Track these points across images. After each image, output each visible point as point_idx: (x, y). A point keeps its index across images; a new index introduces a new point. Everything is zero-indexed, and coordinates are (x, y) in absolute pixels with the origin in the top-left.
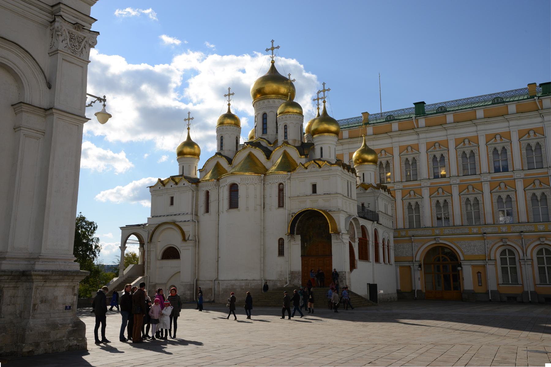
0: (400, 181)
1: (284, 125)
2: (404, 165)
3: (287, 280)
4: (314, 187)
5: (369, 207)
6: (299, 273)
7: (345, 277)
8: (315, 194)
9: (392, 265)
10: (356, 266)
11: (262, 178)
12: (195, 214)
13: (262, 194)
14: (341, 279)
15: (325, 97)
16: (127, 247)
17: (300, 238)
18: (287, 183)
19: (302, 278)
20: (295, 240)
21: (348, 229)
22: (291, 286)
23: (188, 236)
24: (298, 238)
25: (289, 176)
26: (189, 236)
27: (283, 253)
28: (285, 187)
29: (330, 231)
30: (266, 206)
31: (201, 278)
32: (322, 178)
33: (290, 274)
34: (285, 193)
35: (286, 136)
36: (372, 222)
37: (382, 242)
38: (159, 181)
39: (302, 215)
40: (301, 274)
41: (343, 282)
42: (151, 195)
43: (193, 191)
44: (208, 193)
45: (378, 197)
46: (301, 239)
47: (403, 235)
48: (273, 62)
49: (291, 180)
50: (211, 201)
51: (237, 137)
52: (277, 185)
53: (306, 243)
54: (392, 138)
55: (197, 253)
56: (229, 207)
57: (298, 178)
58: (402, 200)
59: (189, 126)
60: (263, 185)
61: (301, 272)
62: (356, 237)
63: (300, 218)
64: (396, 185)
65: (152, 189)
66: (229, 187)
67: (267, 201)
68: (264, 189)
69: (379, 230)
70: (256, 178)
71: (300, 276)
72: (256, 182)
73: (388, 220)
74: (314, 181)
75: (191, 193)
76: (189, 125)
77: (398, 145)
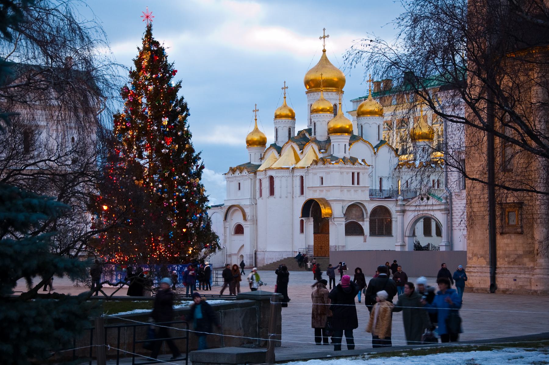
8: (322, 186)
24: (312, 219)
30: (295, 193)
31: (259, 250)
35: (315, 132)
43: (251, 179)
44: (261, 180)
48: (324, 51)
51: (290, 129)
60: (292, 176)
62: (365, 216)
65: (226, 175)
67: (295, 191)
72: (287, 175)
74: (321, 175)
75: (250, 180)
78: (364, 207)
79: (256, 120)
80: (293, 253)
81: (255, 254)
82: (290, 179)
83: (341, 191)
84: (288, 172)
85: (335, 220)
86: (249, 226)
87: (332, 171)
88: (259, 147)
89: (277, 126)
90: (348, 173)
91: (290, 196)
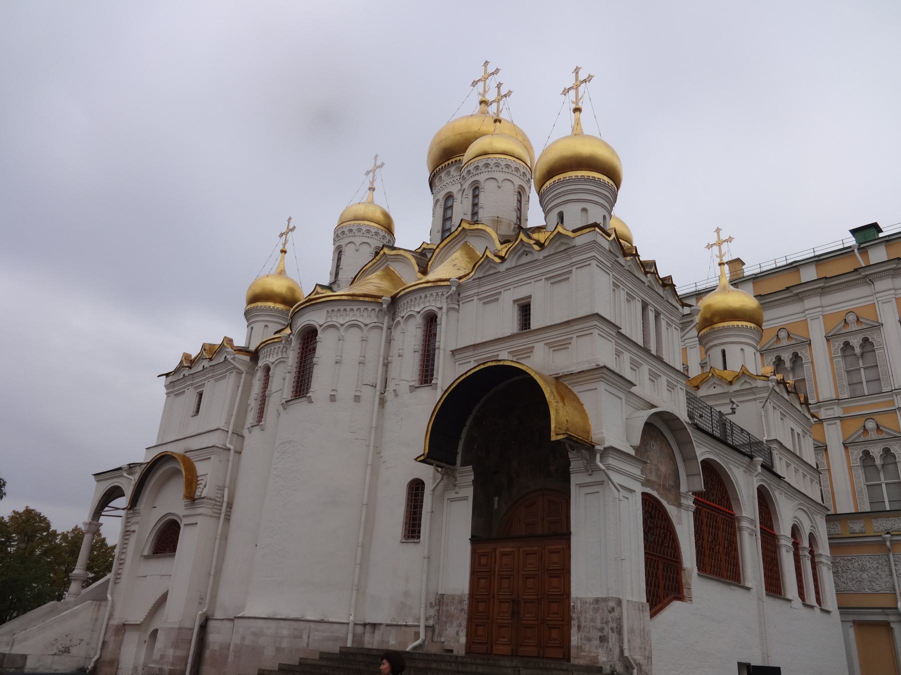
0: (834, 397)
1: (473, 188)
2: (840, 359)
3: (419, 626)
4: (525, 309)
5: (734, 413)
6: (461, 602)
7: (620, 619)
9: (828, 612)
10: (685, 594)
11: (385, 306)
12: (233, 433)
13: (382, 353)
14: (602, 629)
15: (580, 97)
16: (102, 524)
17: (472, 478)
18: (449, 310)
19: (470, 620)
20: (455, 486)
21: (637, 441)
22: (434, 649)
23: (202, 486)
24: (466, 477)
25: (454, 288)
26: (205, 486)
27: (419, 532)
28: (441, 324)
29: (553, 434)
30: (391, 386)
31: (218, 615)
32: (546, 279)
33: (436, 605)
34: (440, 342)
36: (747, 459)
37: (789, 534)
38: (183, 359)
39: (482, 401)
40: (466, 607)
41: (611, 645)
42: (167, 394)
43: (240, 373)
44: (267, 369)
45: (767, 401)
46: (475, 482)
47: (857, 531)
49: (461, 303)
50: (273, 391)
52: (419, 320)
53: (497, 498)
54: (803, 301)
55: (218, 537)
56: (291, 394)
57: (478, 294)
58: (844, 444)
59: (284, 247)
60: (389, 328)
61: (466, 599)
62: (683, 488)
63: (474, 412)
64: (822, 409)
65: (170, 379)
66: (299, 342)
67: (393, 372)
68: (389, 341)
69: (777, 496)
70: (370, 309)
71: (463, 613)
72: (367, 322)
73: (804, 476)
74: (521, 293)
76: (284, 245)
77: (821, 313)
78: (685, 444)
79: (284, 252)
80: (359, 630)
81: (203, 627)
82: (377, 339)
83: (618, 354)
84: (373, 314)
85: (611, 461)
86: (198, 520)
87: (583, 264)
88: (280, 306)
89: (343, 242)
90: (630, 298)
91: (370, 396)
